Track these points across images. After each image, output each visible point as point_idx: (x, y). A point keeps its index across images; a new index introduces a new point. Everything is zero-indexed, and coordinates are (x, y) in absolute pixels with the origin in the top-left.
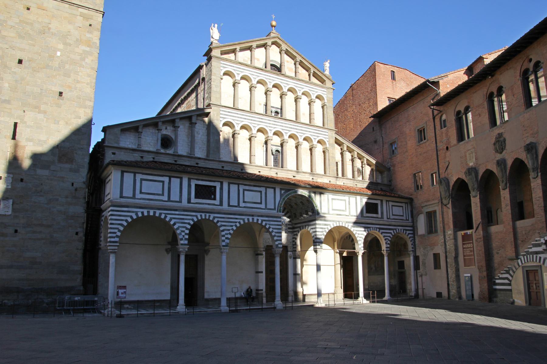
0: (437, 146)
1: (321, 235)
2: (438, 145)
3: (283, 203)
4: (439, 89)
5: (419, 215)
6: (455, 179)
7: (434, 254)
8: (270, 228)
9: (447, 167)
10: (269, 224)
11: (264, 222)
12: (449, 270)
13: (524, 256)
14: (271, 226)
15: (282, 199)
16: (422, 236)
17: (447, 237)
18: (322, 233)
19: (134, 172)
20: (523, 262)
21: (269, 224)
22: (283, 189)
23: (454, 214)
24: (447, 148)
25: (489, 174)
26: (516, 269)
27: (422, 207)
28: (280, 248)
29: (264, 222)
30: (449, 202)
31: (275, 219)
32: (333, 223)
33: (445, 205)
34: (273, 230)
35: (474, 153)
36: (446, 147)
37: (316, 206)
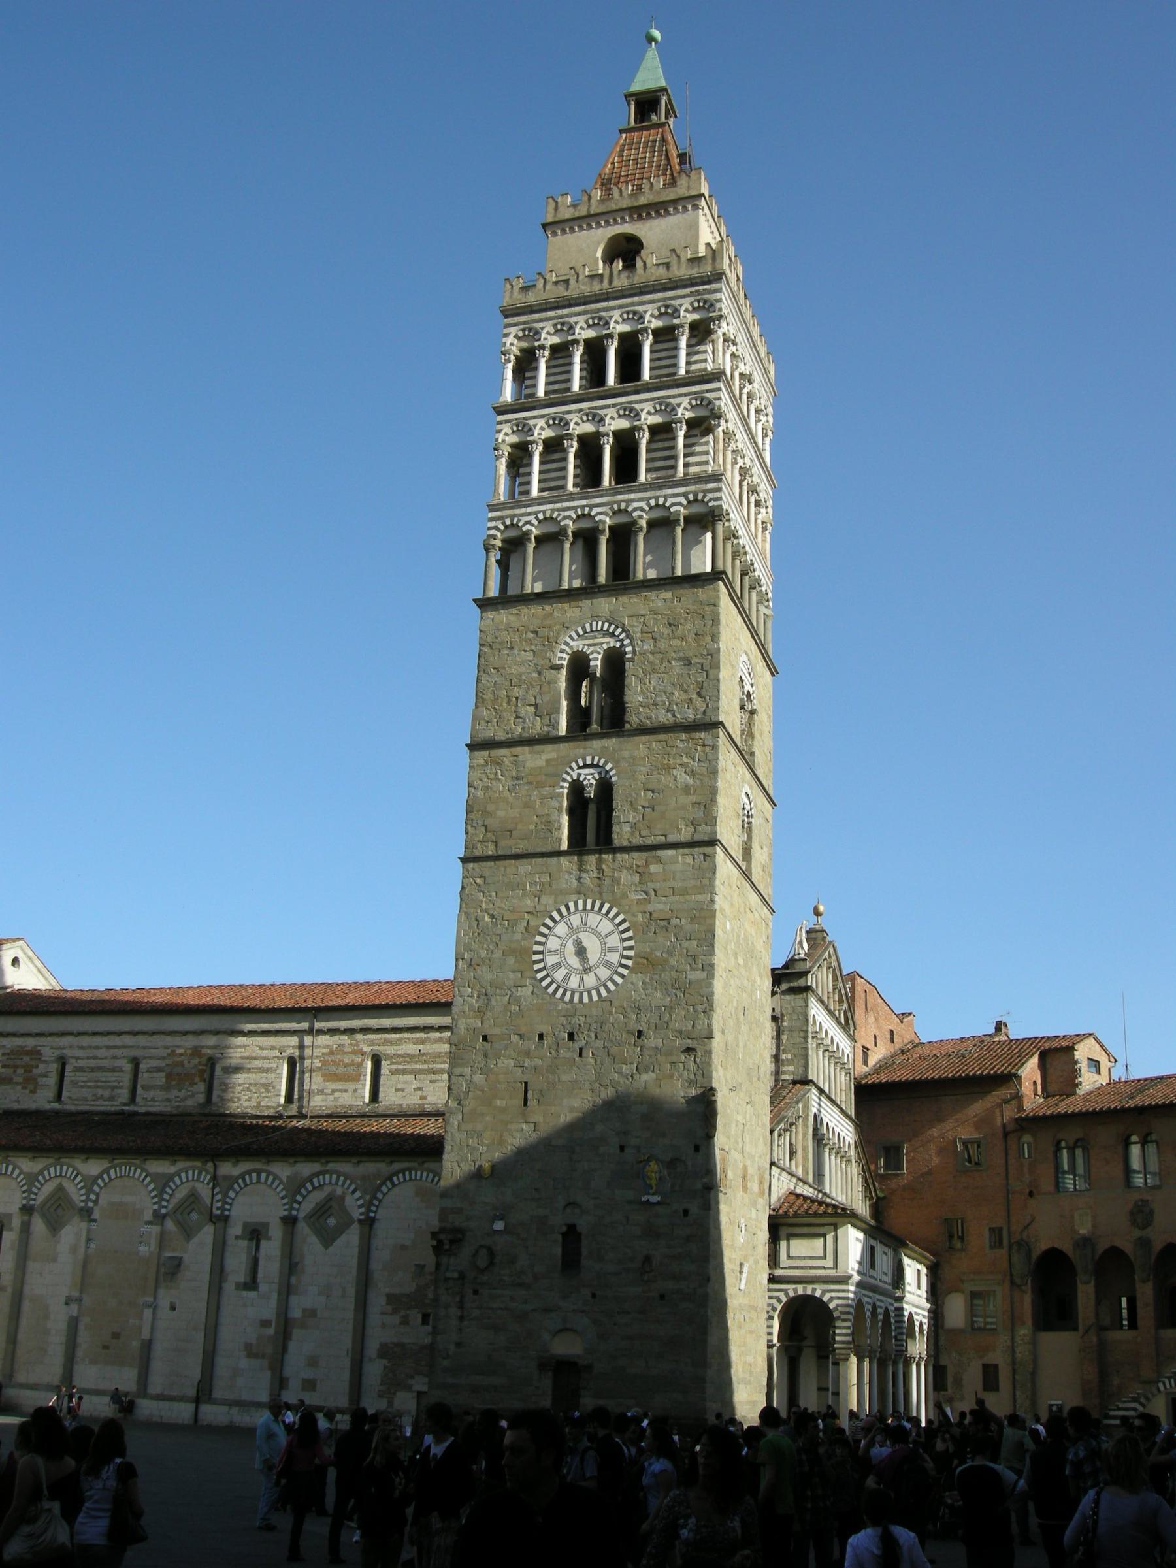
0: (1007, 1184)
2: (1010, 1181)
4: (1021, 1088)
5: (950, 1293)
6: (1044, 1246)
7: (984, 1365)
9: (1028, 1225)
12: (1018, 1393)
13: (1169, 1378)
16: (954, 1331)
17: (1018, 1339)
19: (798, 1217)
20: (1168, 1387)
23: (1033, 1302)
24: (1031, 1194)
25: (1114, 1253)
26: (1154, 1395)
27: (962, 1281)
30: (1026, 1284)
33: (1019, 1286)
35: (1090, 1219)
36: (1028, 1191)
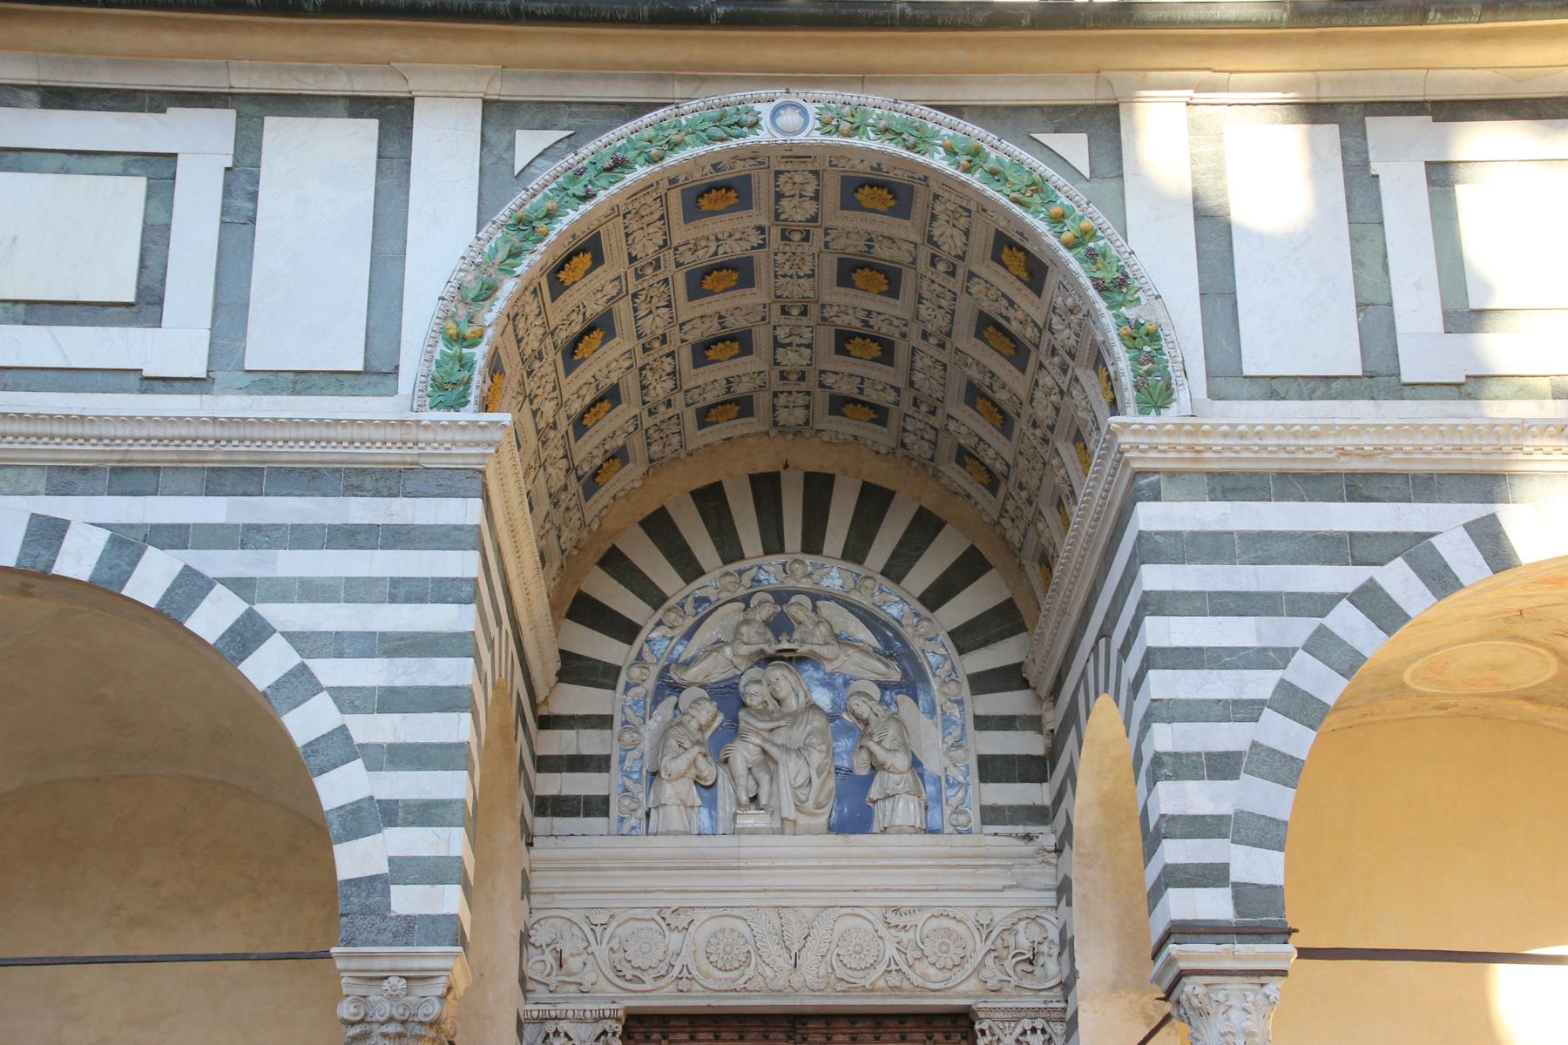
1: (1247, 710)
3: (509, 287)
8: (250, 633)
10: (241, 586)
11: (151, 551)
14: (267, 610)
15: (496, 236)
18: (1260, 684)
21: (241, 586)
22: (544, 113)
28: (409, 929)
29: (151, 551)
31: (361, 510)
32: (1476, 511)
34: (308, 662)
37: (1118, 286)
